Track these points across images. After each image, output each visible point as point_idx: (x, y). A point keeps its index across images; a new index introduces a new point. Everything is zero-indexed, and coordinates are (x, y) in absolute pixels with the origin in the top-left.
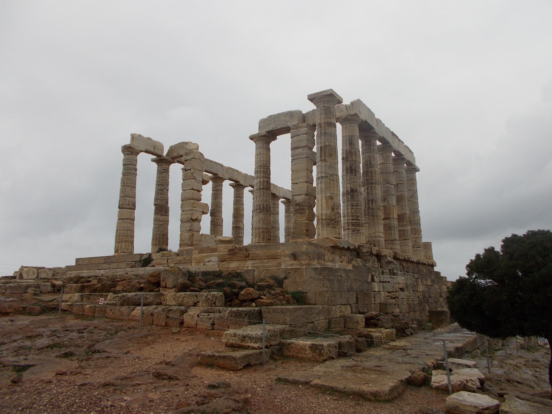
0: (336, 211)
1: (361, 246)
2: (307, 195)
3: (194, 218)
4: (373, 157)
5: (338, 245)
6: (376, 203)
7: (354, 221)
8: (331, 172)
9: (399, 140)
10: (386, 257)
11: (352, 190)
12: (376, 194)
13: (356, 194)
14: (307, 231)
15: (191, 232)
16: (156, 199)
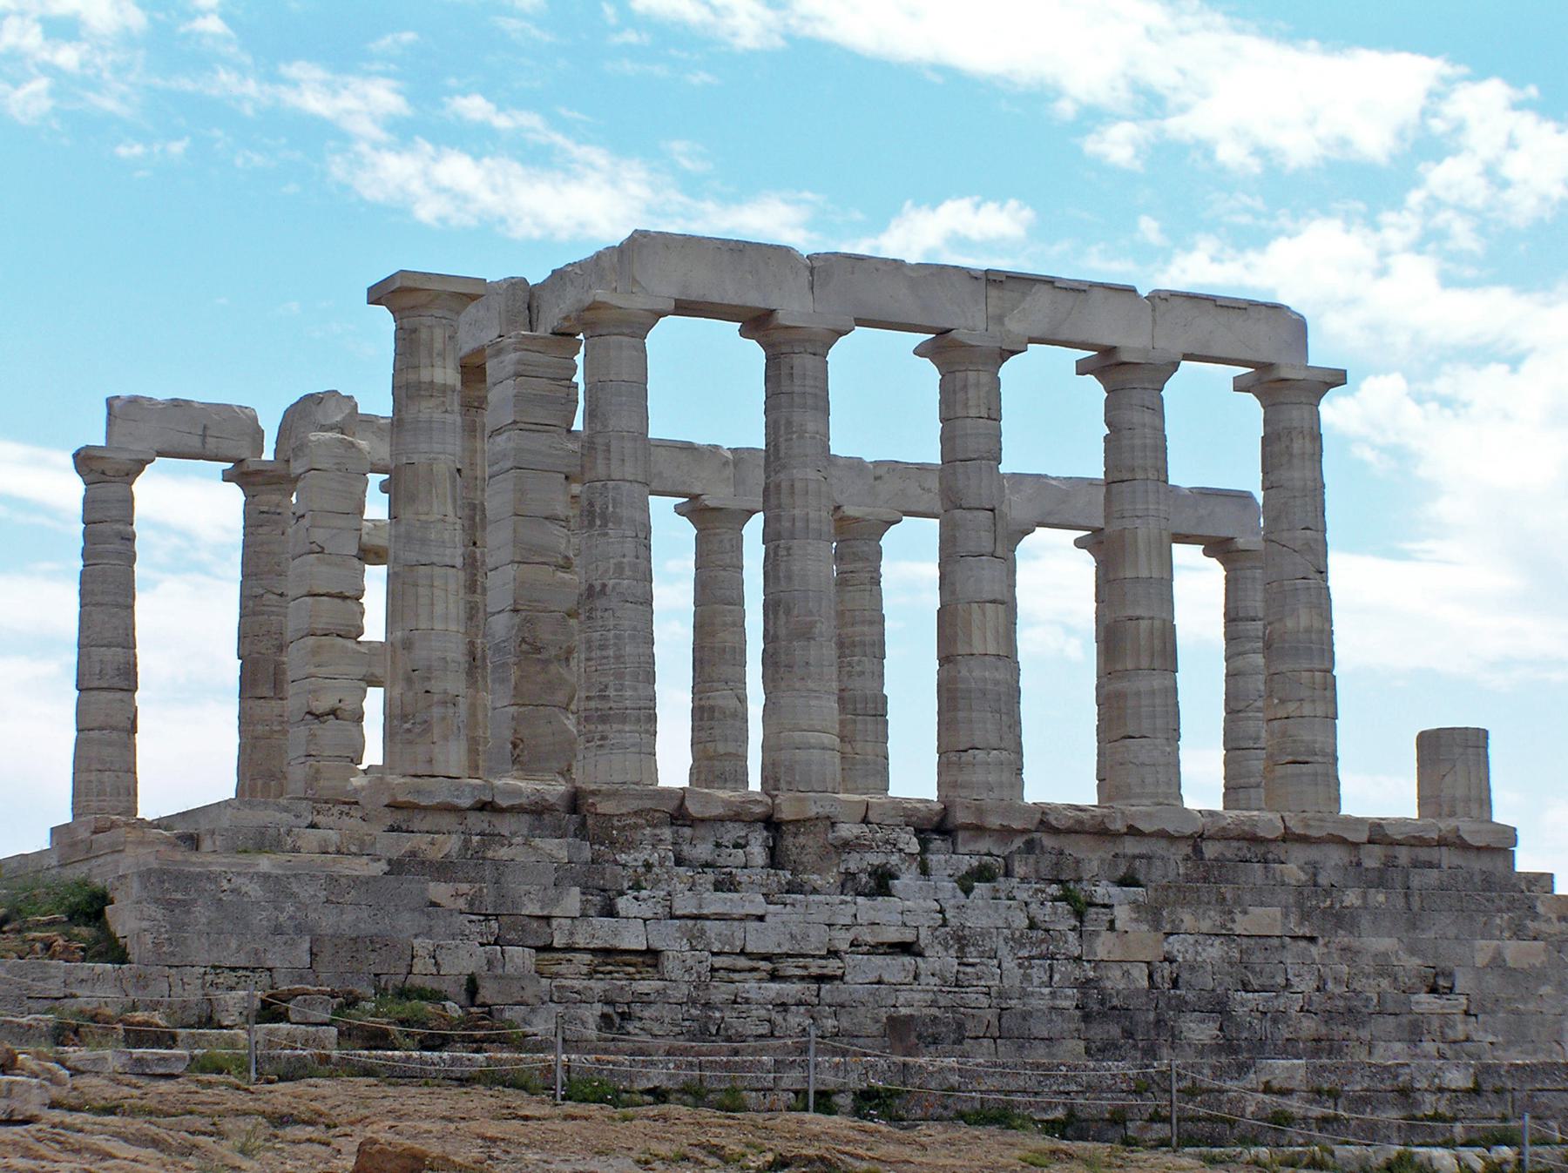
0: (419, 687)
1: (593, 793)
2: (516, 611)
3: (324, 704)
4: (789, 423)
5: (401, 798)
6: (788, 612)
7: (593, 704)
8: (412, 557)
9: (1079, 290)
10: (833, 824)
11: (591, 587)
12: (789, 578)
13: (600, 603)
14: (515, 746)
15: (311, 761)
16: (242, 636)
